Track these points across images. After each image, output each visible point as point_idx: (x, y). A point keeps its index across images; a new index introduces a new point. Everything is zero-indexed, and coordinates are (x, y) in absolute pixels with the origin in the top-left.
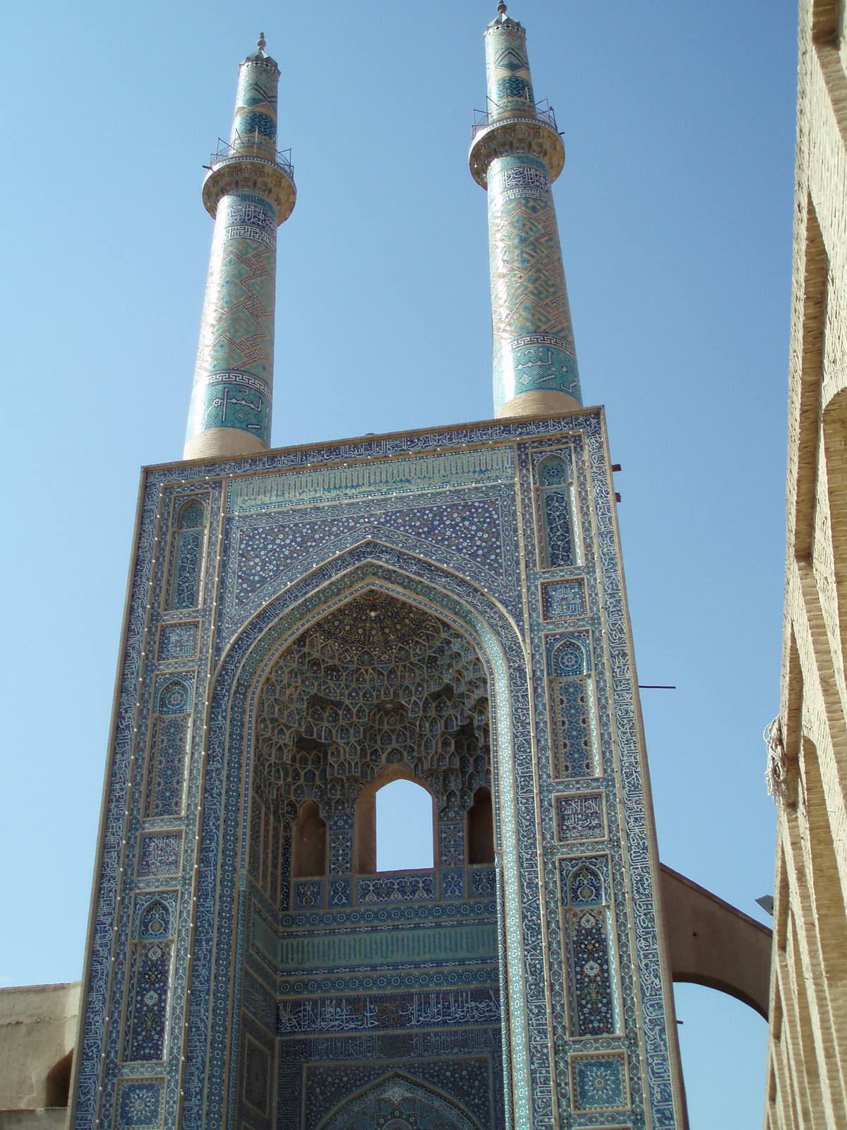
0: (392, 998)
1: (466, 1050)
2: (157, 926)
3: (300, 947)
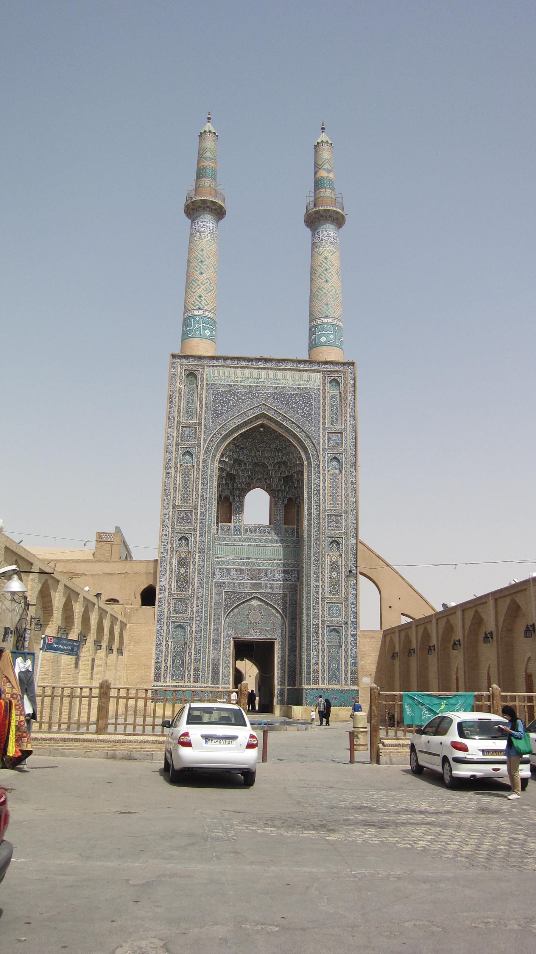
0: (254, 570)
2: (183, 545)
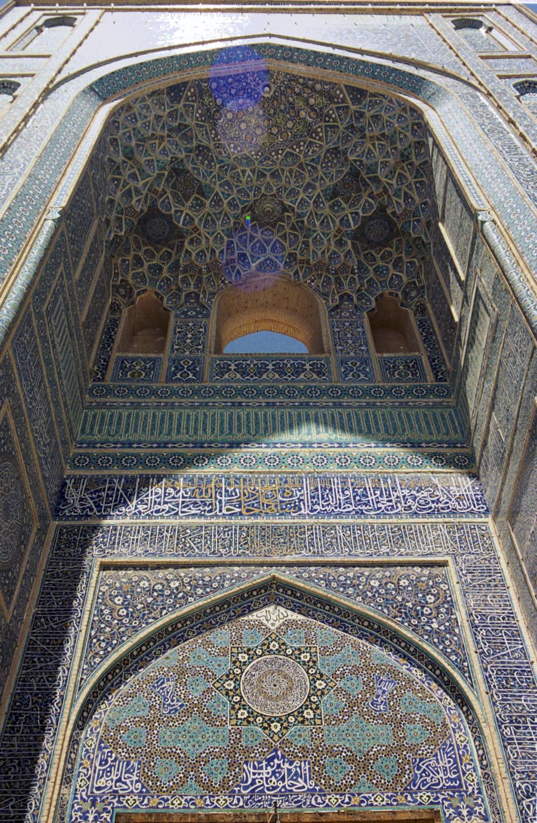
1: (402, 550)
3: (115, 419)
